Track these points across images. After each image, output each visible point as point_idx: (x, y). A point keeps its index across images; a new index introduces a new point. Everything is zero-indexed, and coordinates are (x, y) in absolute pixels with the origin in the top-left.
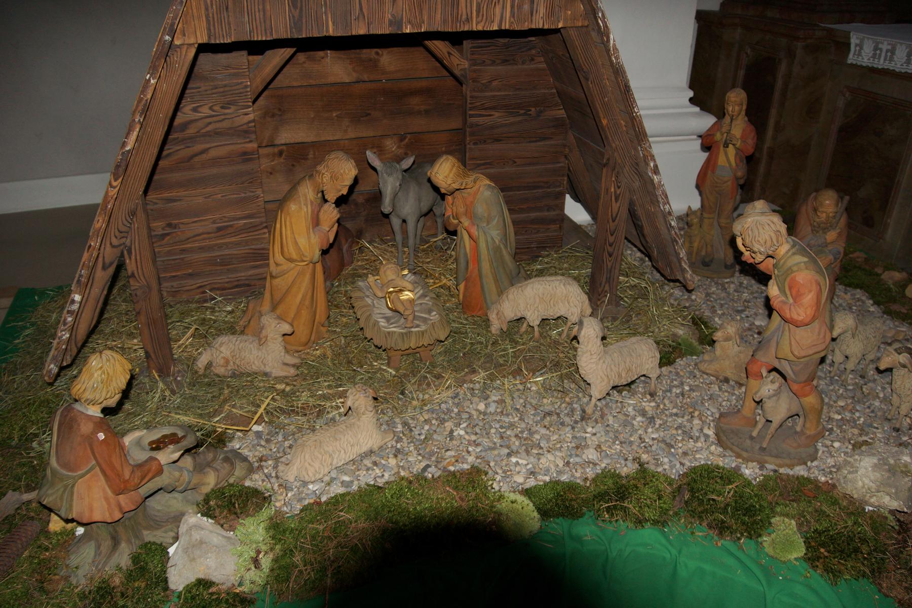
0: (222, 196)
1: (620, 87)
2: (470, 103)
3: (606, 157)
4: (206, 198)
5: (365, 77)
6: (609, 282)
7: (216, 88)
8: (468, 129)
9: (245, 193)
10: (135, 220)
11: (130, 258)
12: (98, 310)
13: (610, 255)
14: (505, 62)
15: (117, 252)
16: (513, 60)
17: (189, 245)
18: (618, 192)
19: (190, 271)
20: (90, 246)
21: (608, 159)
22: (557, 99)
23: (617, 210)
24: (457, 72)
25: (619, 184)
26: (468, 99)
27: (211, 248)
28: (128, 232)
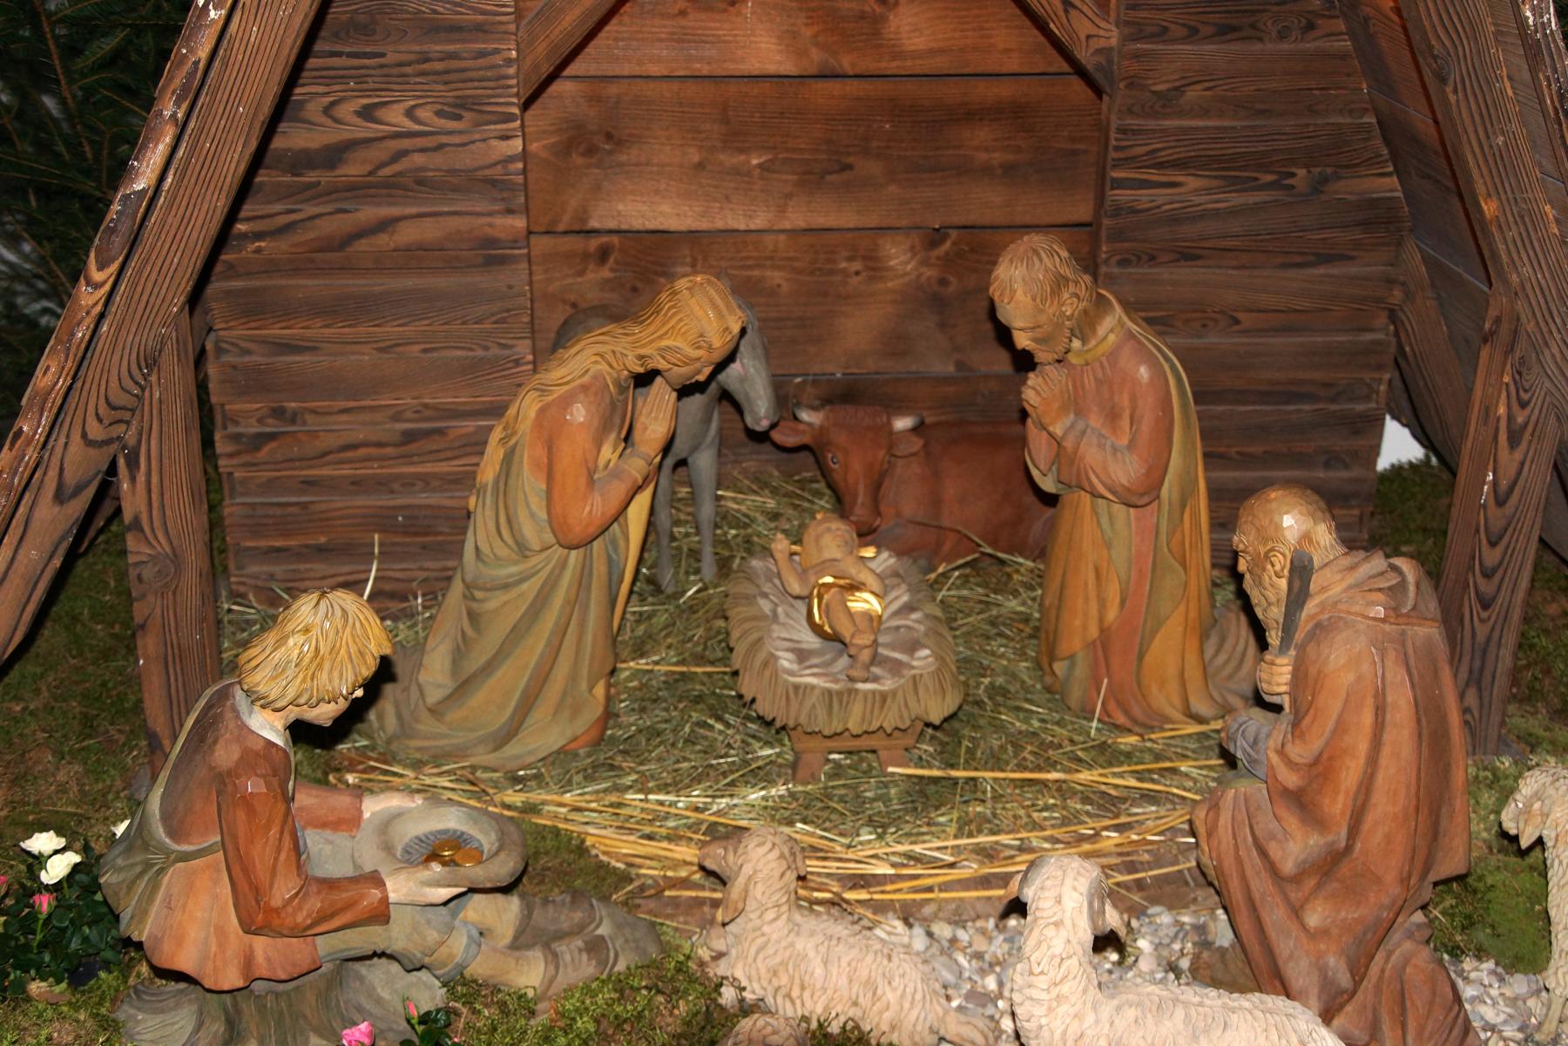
0: (425, 351)
1: (1541, 102)
2: (1117, 148)
3: (1493, 312)
4: (380, 350)
5: (846, 63)
6: (1479, 683)
7: (428, 60)
8: (1106, 222)
9: (486, 348)
10: (153, 378)
11: (133, 479)
12: (32, 608)
13: (1486, 605)
14: (1225, 31)
15: (101, 459)
16: (1253, 26)
17: (326, 472)
18: (1520, 420)
19: (323, 540)
20: (20, 431)
21: (1498, 321)
22: (1378, 142)
23: (1513, 471)
24: (1084, 55)
25: (1525, 397)
26: (1113, 135)
27: (382, 484)
28: (133, 410)
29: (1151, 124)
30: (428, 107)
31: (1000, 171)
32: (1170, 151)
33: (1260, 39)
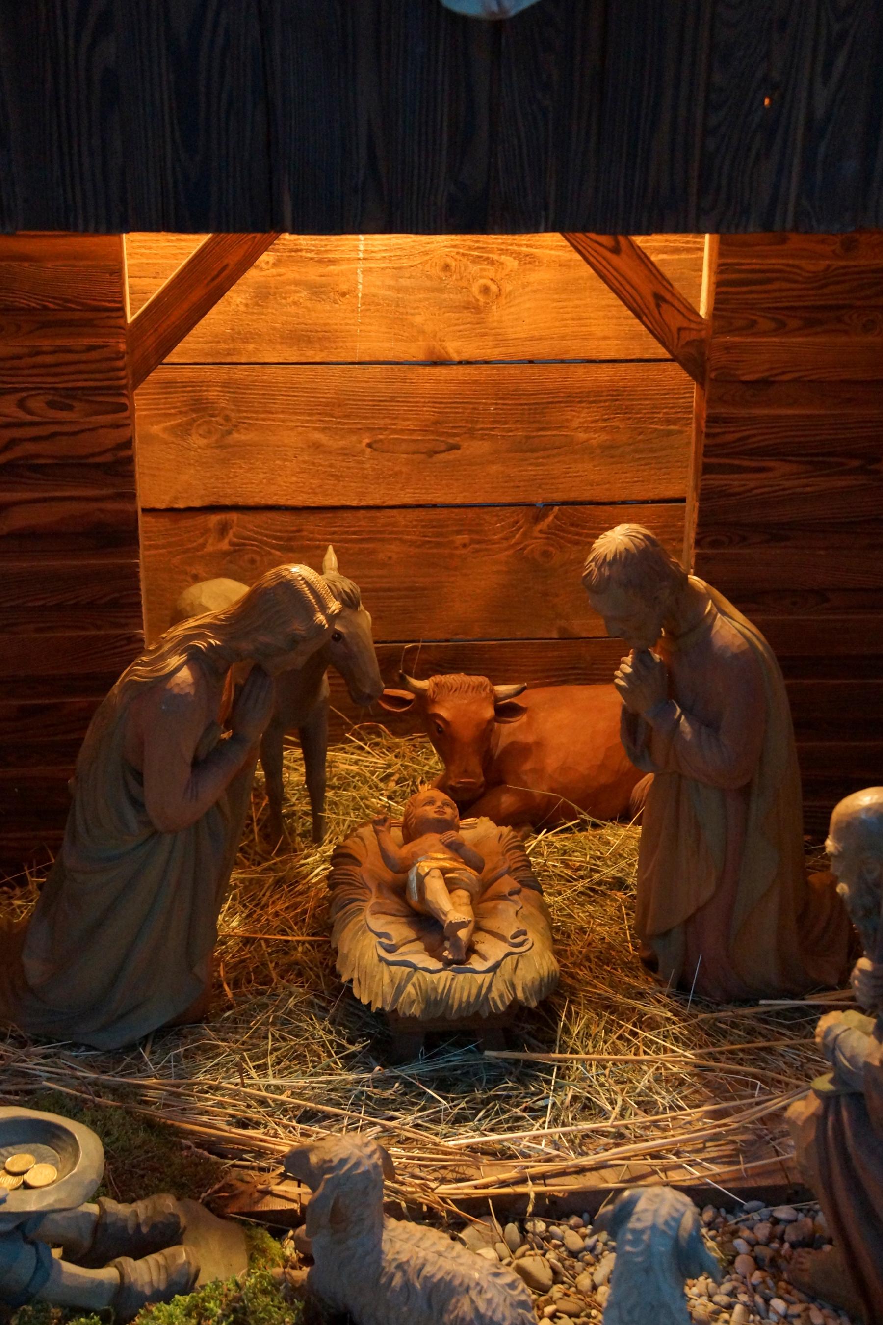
7: (38, 353)
29: (744, 412)
30: (41, 397)
31: (598, 451)
32: (761, 438)
33: (846, 332)
